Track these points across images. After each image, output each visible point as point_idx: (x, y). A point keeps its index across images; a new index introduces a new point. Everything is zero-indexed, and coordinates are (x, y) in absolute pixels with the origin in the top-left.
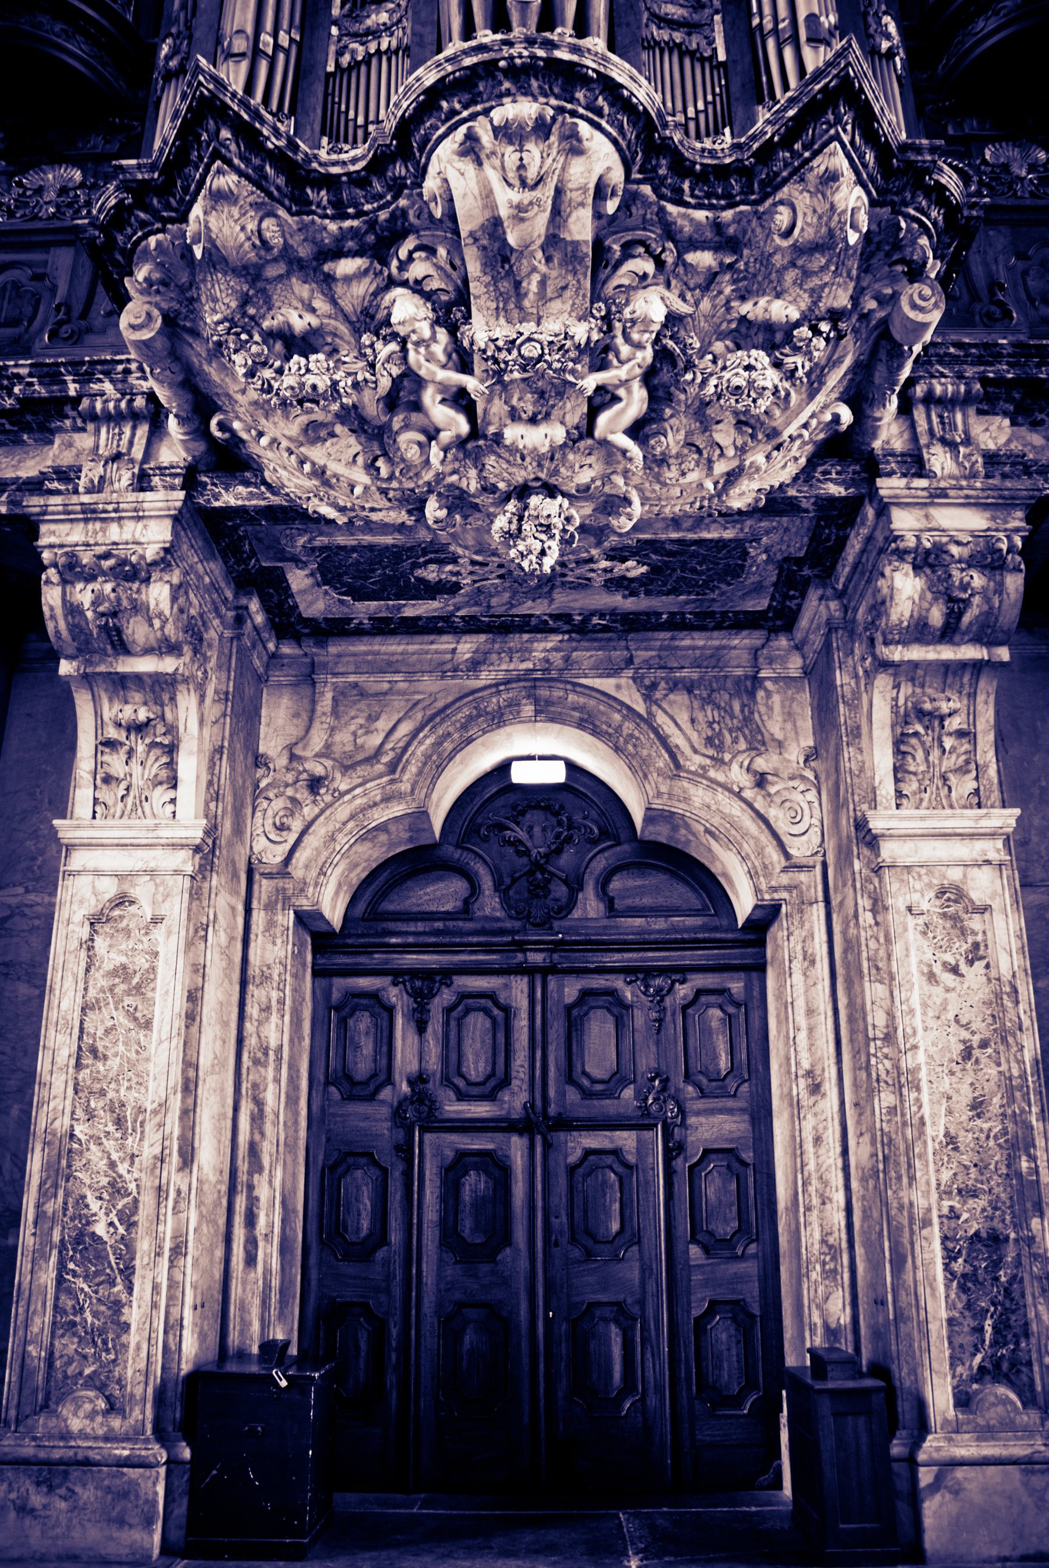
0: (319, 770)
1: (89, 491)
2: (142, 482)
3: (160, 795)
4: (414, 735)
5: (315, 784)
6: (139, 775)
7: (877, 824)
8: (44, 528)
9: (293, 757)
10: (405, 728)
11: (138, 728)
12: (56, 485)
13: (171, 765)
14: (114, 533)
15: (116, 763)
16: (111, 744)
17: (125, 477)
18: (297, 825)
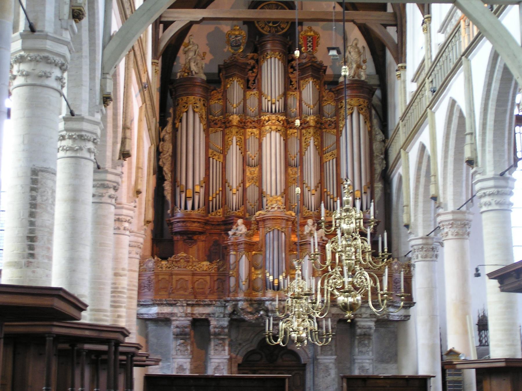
0: (240, 342)
1: (217, 317)
2: (224, 317)
3: (223, 352)
4: (254, 337)
5: (240, 344)
6: (220, 349)
7: (318, 357)
8: (211, 322)
9: (237, 340)
10: (253, 336)
11: (221, 344)
12: (211, 315)
13: (224, 348)
14: (221, 323)
15: (217, 348)
16: (217, 345)
17: (222, 316)
18: (238, 350)
